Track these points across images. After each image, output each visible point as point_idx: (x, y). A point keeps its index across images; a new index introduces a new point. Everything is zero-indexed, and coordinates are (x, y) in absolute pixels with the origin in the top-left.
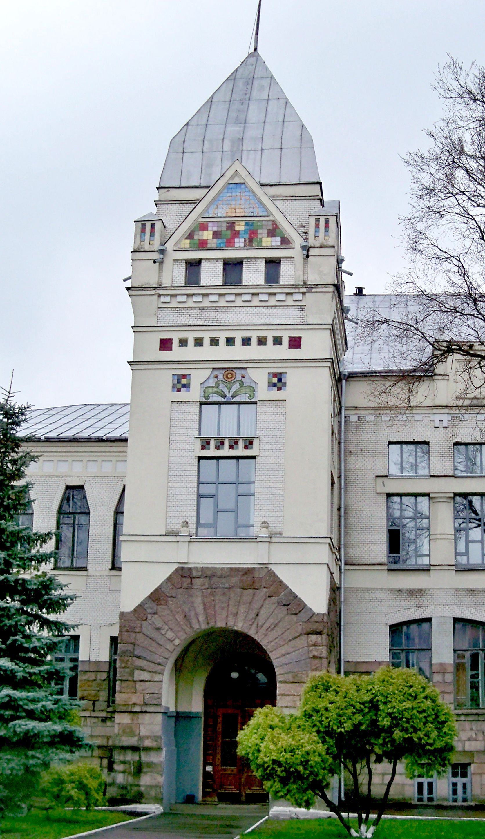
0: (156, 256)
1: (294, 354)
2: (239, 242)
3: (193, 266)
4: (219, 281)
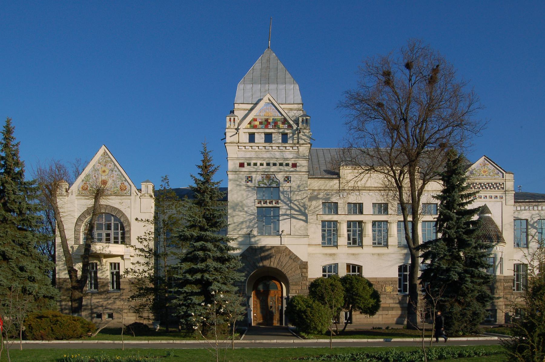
2: (270, 127)
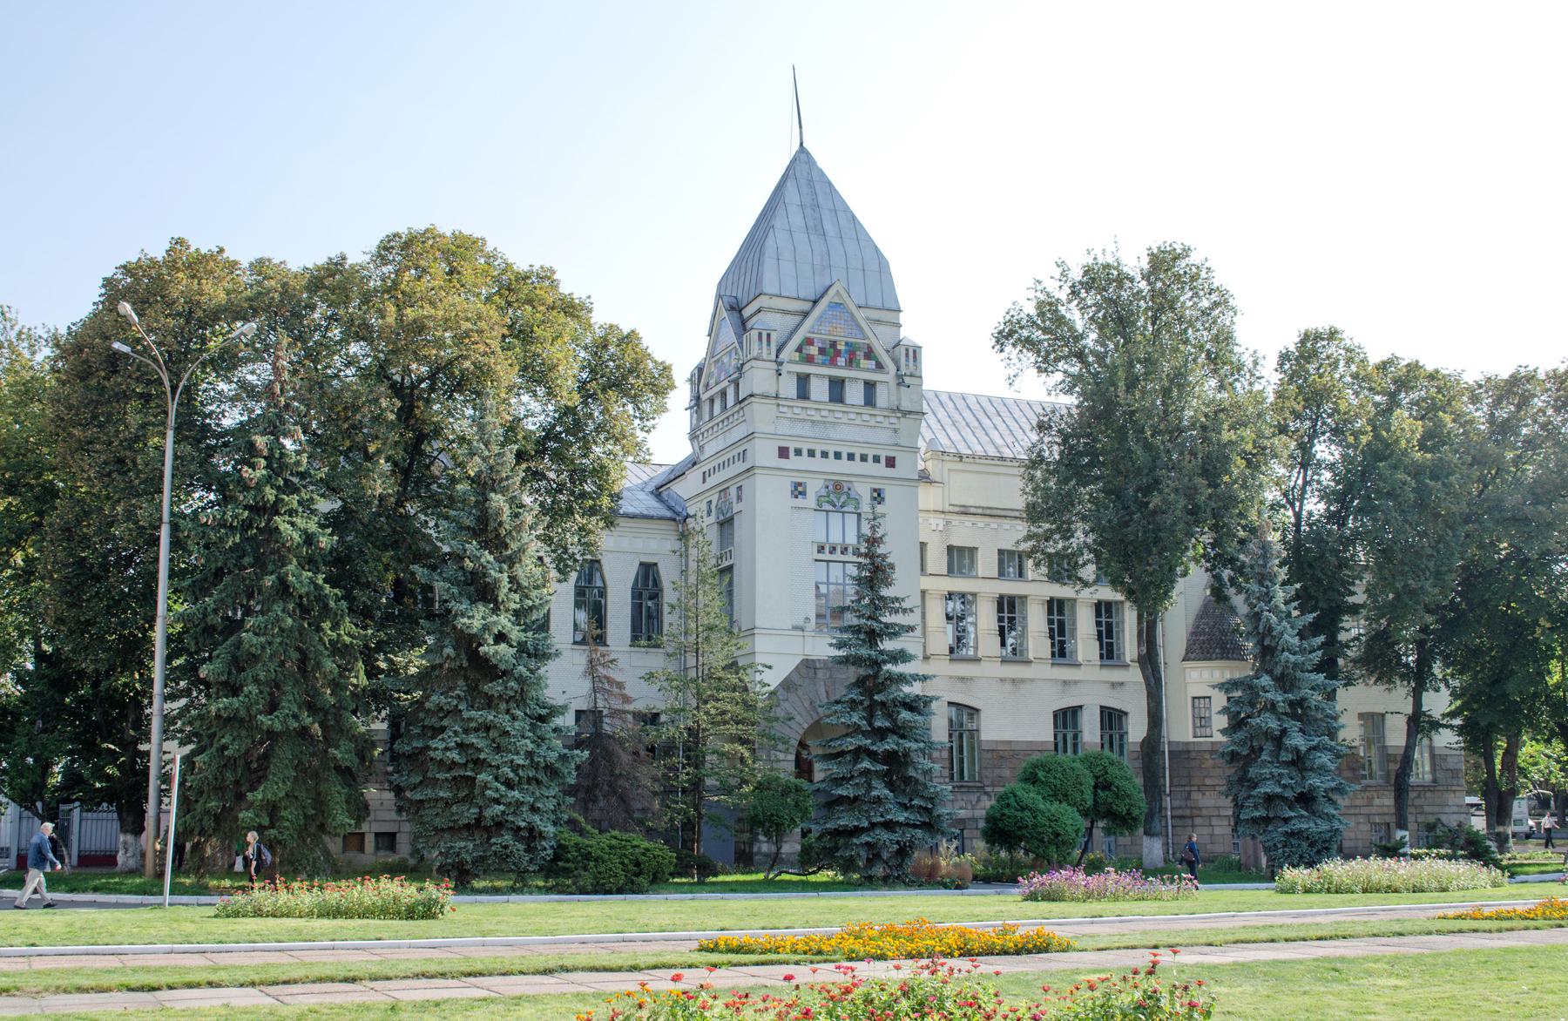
0: (774, 366)
1: (890, 472)
2: (841, 361)
3: (803, 380)
4: (826, 397)
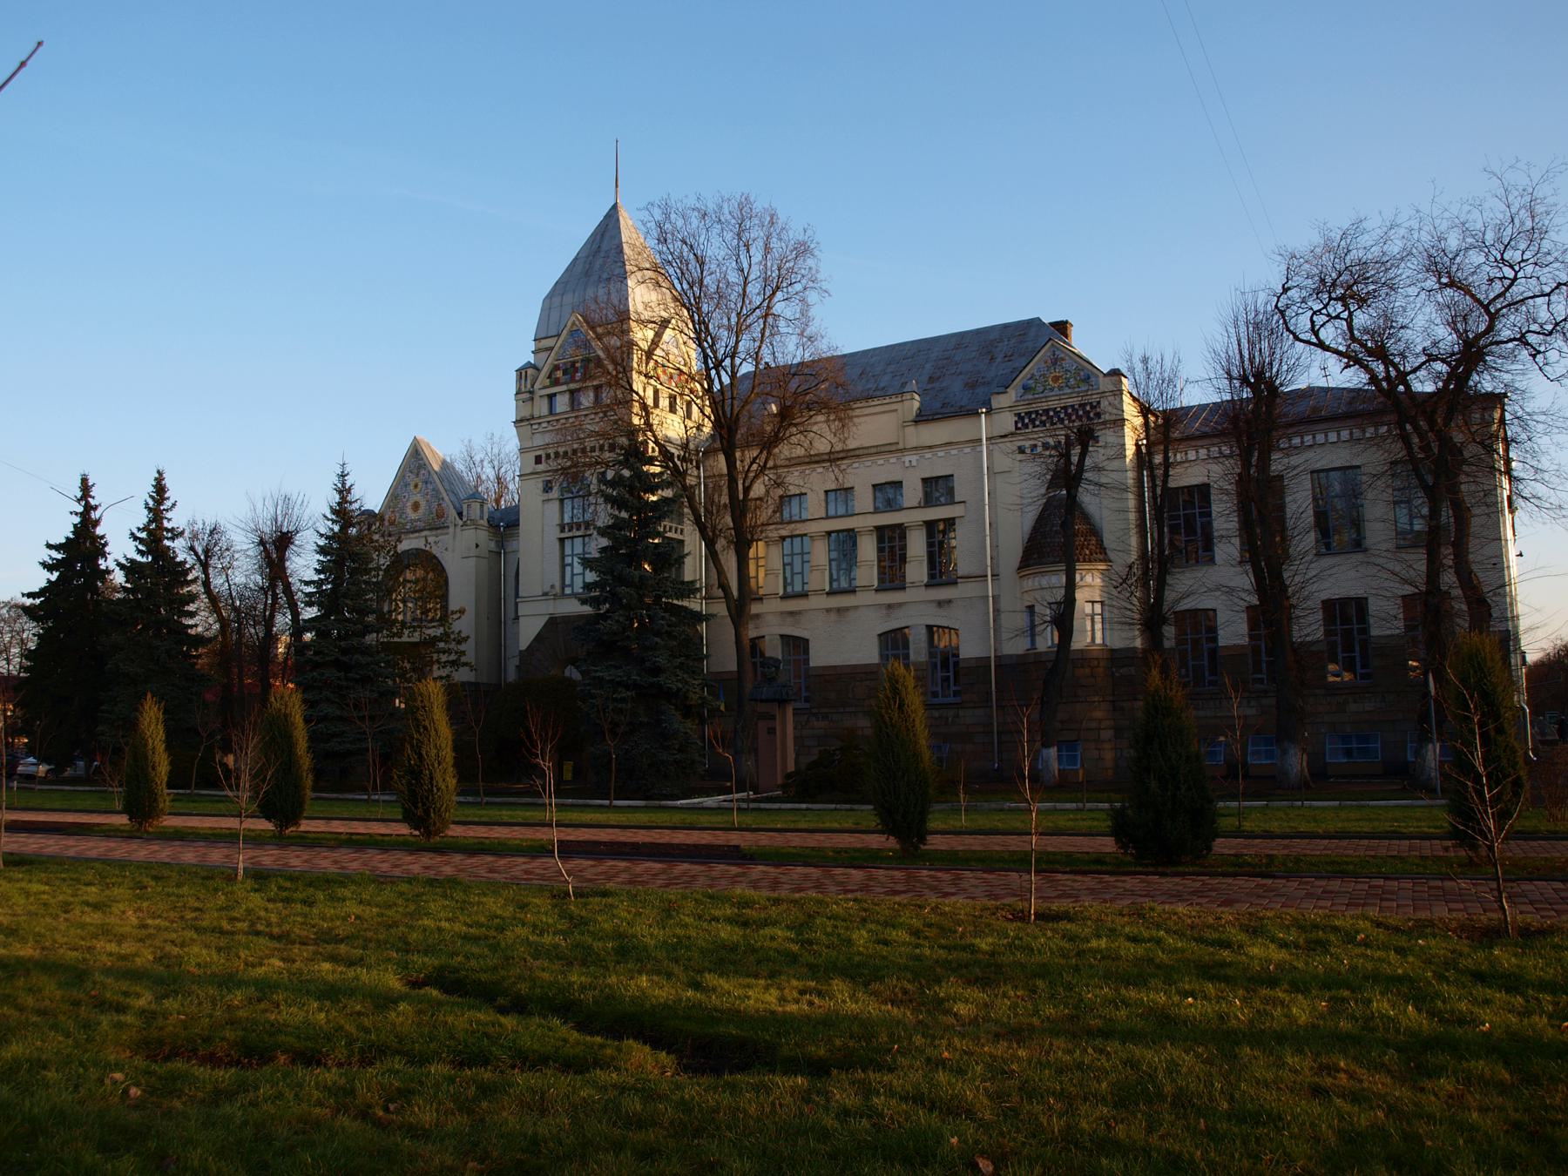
3: (551, 397)
